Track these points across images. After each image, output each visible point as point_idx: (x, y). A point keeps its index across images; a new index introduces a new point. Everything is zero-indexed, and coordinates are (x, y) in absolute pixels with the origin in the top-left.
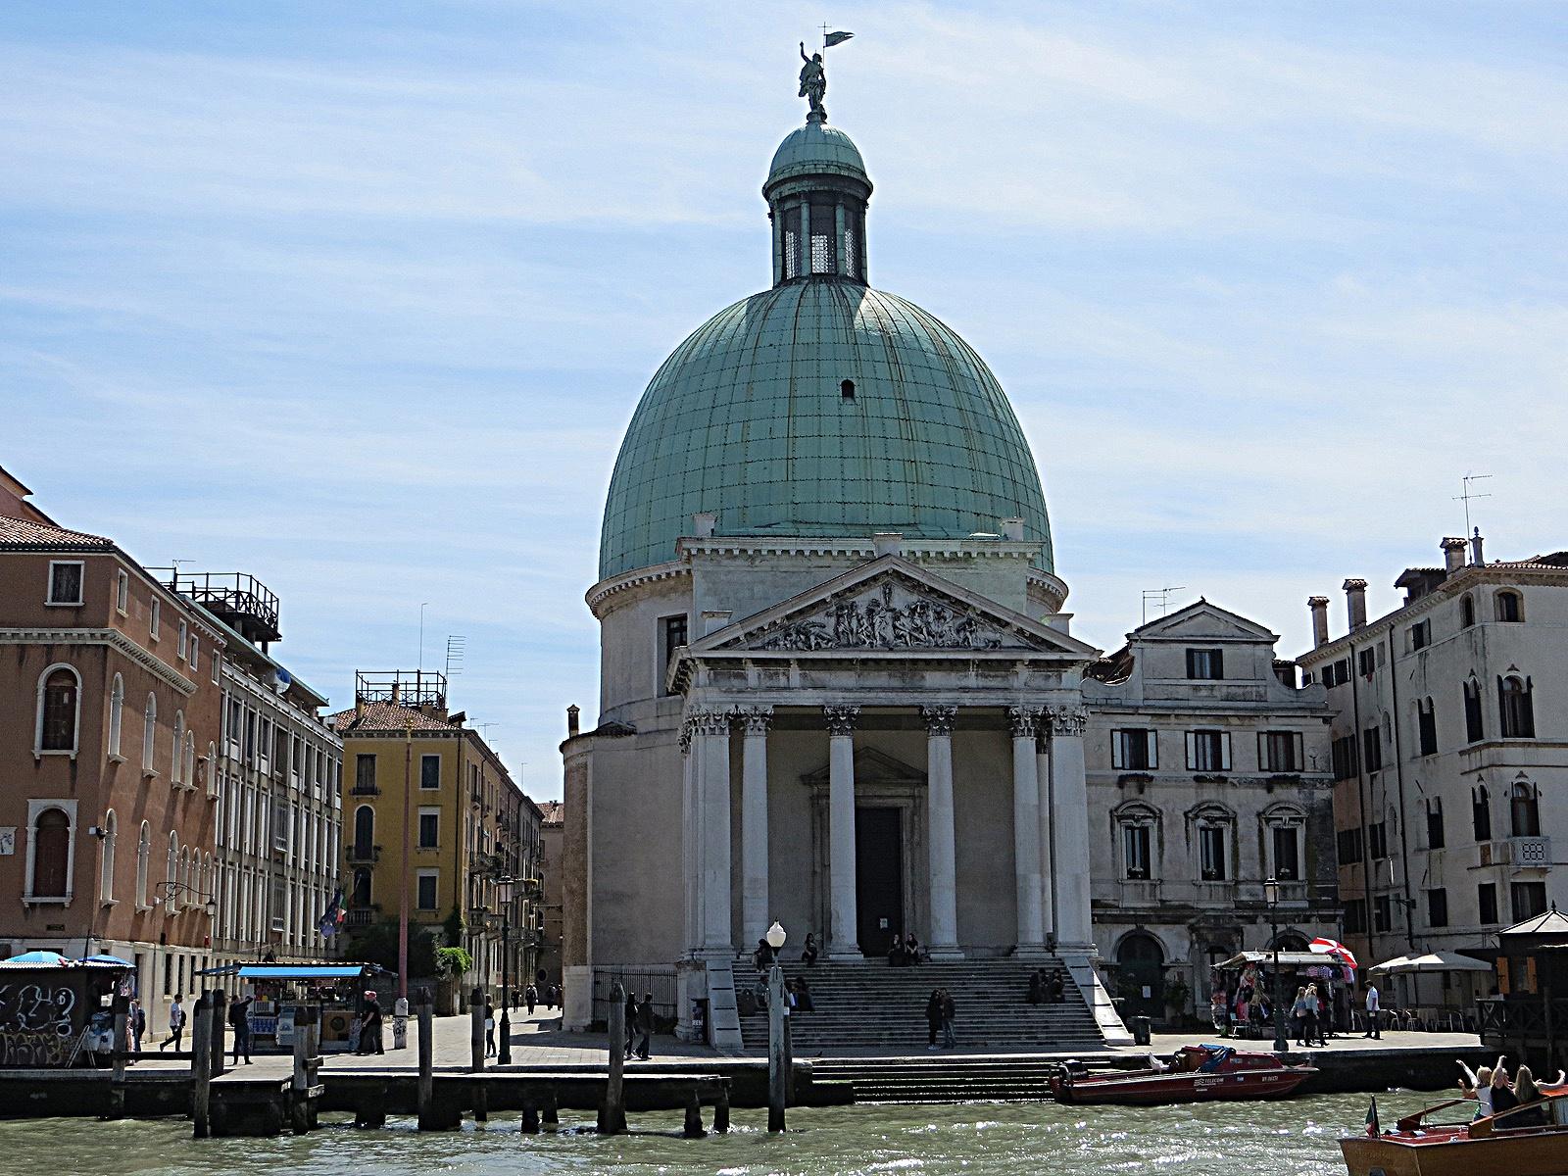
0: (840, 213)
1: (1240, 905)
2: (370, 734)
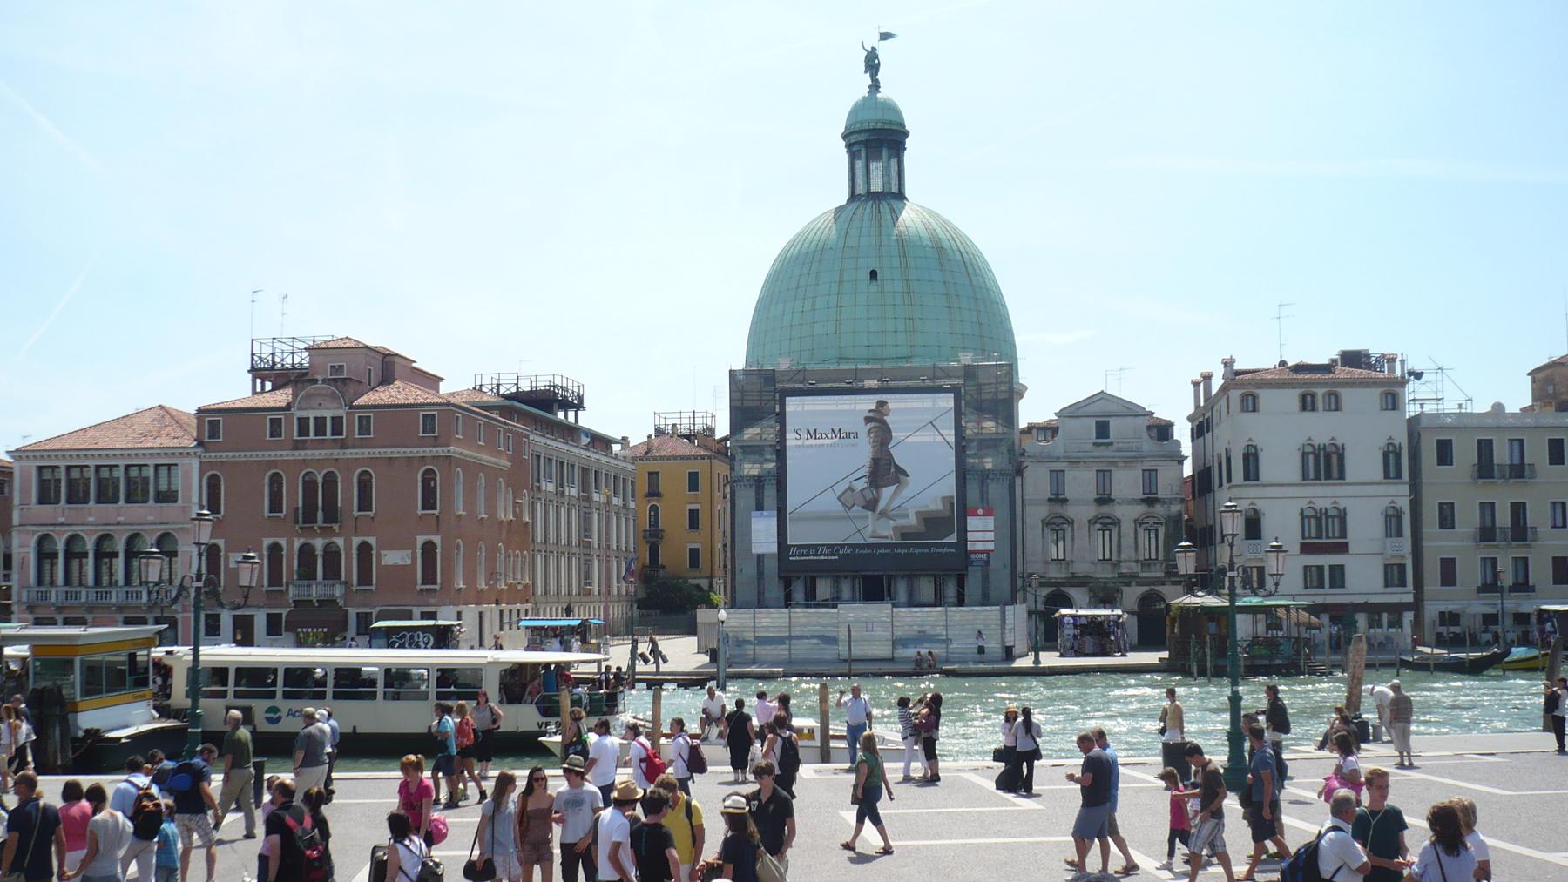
0: (885, 152)
1: (1121, 575)
2: (655, 459)
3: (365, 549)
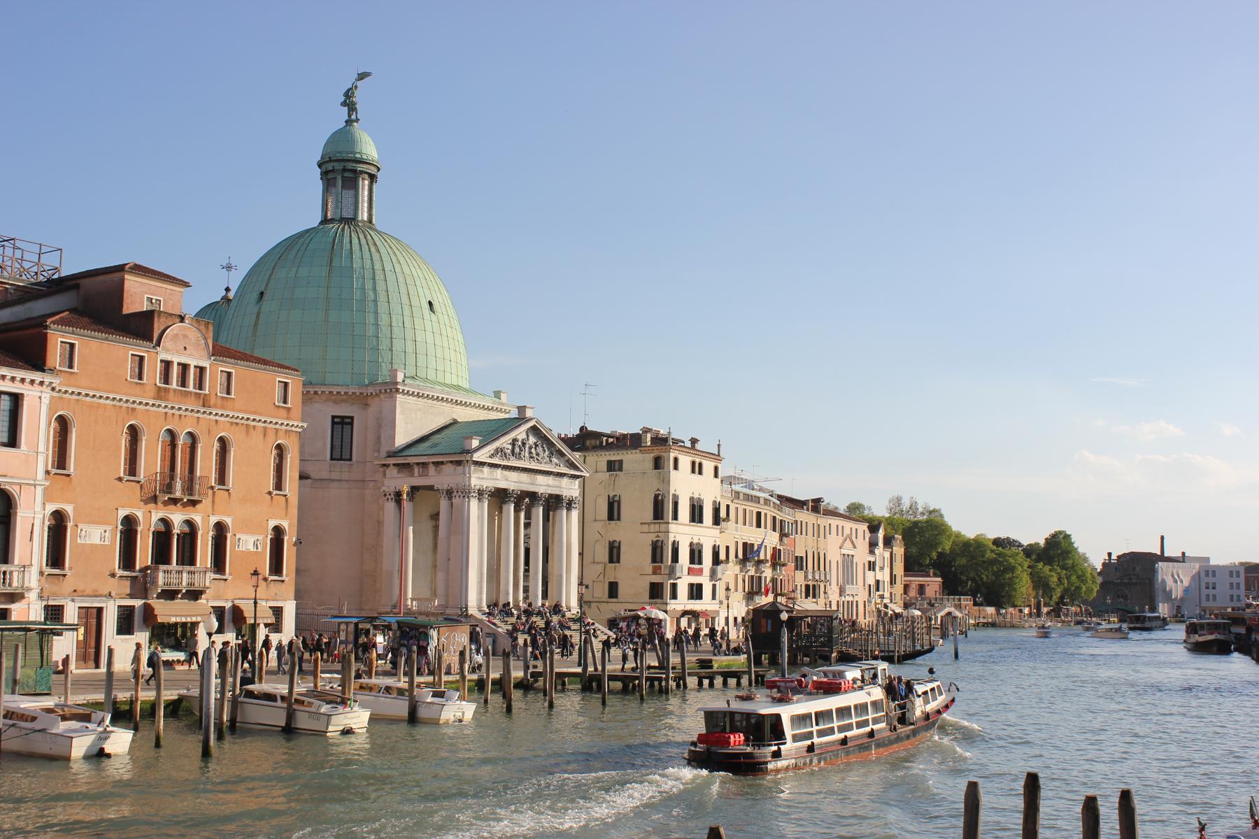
3: (220, 529)
